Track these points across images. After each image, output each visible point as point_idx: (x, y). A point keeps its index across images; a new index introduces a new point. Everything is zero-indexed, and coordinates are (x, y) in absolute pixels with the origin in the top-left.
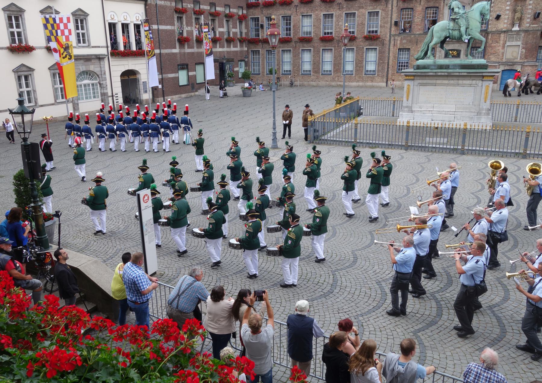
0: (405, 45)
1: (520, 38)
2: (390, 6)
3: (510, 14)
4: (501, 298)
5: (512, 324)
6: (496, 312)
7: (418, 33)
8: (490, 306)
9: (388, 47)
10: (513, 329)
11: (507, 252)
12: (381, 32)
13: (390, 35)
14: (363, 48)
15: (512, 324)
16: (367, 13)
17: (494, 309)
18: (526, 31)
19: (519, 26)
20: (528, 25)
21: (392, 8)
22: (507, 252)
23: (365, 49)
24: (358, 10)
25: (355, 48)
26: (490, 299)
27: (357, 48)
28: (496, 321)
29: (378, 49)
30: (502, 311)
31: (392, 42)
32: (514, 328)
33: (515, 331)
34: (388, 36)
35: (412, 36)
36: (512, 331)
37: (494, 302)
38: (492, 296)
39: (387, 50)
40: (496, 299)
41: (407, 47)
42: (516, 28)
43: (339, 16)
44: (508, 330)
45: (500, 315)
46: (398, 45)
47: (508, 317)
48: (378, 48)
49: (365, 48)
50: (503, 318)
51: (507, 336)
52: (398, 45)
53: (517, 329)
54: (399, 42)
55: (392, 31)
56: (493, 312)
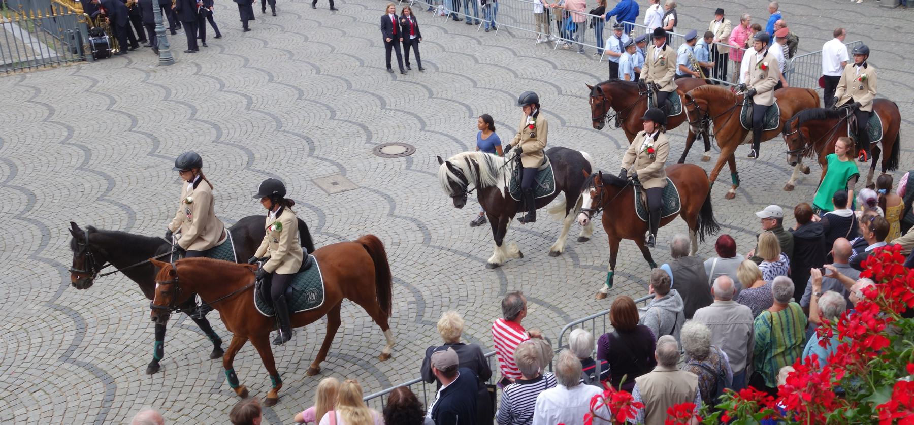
4: (74, 332)
5: (114, 363)
6: (80, 359)
8: (63, 356)
10: (121, 370)
11: (37, 252)
15: (114, 363)
17: (74, 356)
22: (37, 252)
26: (56, 344)
28: (87, 372)
30: (88, 351)
32: (121, 366)
33: (126, 370)
36: (121, 373)
37: (65, 346)
38: (56, 337)
40: (66, 338)
44: (115, 376)
45: (88, 360)
47: (102, 356)
50: (96, 362)
51: (119, 386)
53: (127, 364)
56: (74, 361)
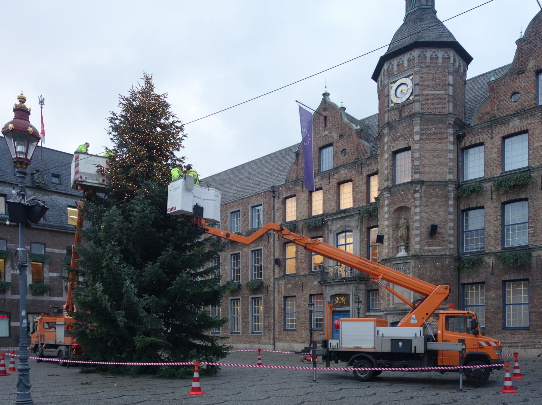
0: (290, 292)
1: (409, 269)
2: (272, 241)
3: (391, 232)
7: (302, 273)
9: (272, 295)
12: (264, 276)
13: (274, 279)
14: (248, 297)
16: (250, 252)
18: (416, 257)
19: (407, 249)
20: (418, 246)
21: (274, 243)
23: (250, 299)
24: (241, 250)
25: (240, 297)
27: (242, 298)
29: (262, 298)
31: (277, 289)
34: (272, 280)
35: (297, 279)
39: (272, 299)
41: (293, 294)
42: (402, 253)
43: (226, 258)
46: (283, 291)
48: (262, 296)
49: (250, 297)
52: (283, 291)
54: (283, 288)
55: (276, 274)
